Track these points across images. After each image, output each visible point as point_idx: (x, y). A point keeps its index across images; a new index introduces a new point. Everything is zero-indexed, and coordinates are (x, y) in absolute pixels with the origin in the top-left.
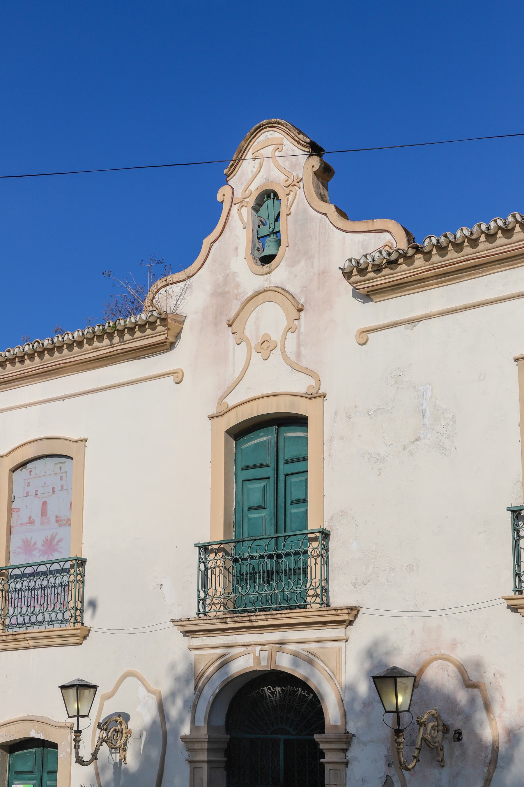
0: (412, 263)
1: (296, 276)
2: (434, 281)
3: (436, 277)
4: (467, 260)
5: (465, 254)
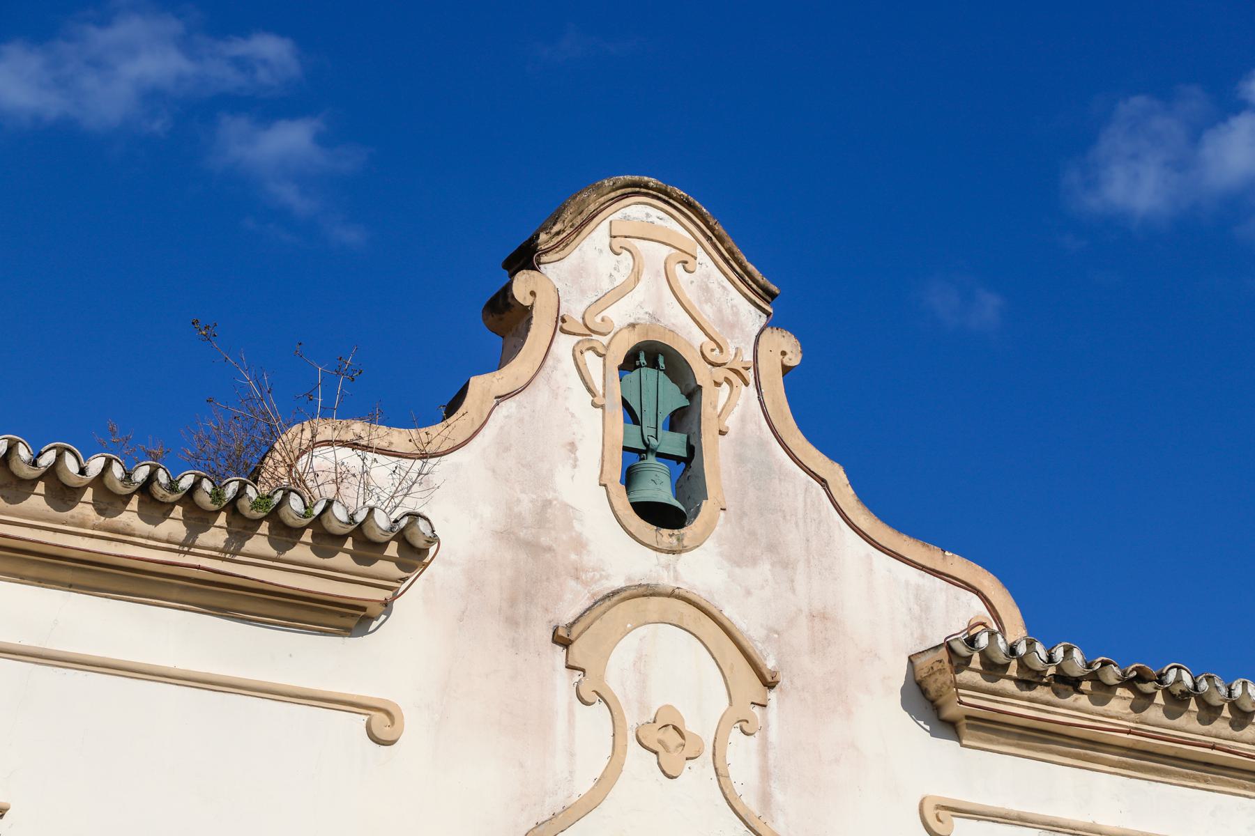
0: (1104, 702)
1: (748, 593)
2: (1116, 758)
3: (1124, 752)
4: (1213, 748)
5: (1214, 732)
